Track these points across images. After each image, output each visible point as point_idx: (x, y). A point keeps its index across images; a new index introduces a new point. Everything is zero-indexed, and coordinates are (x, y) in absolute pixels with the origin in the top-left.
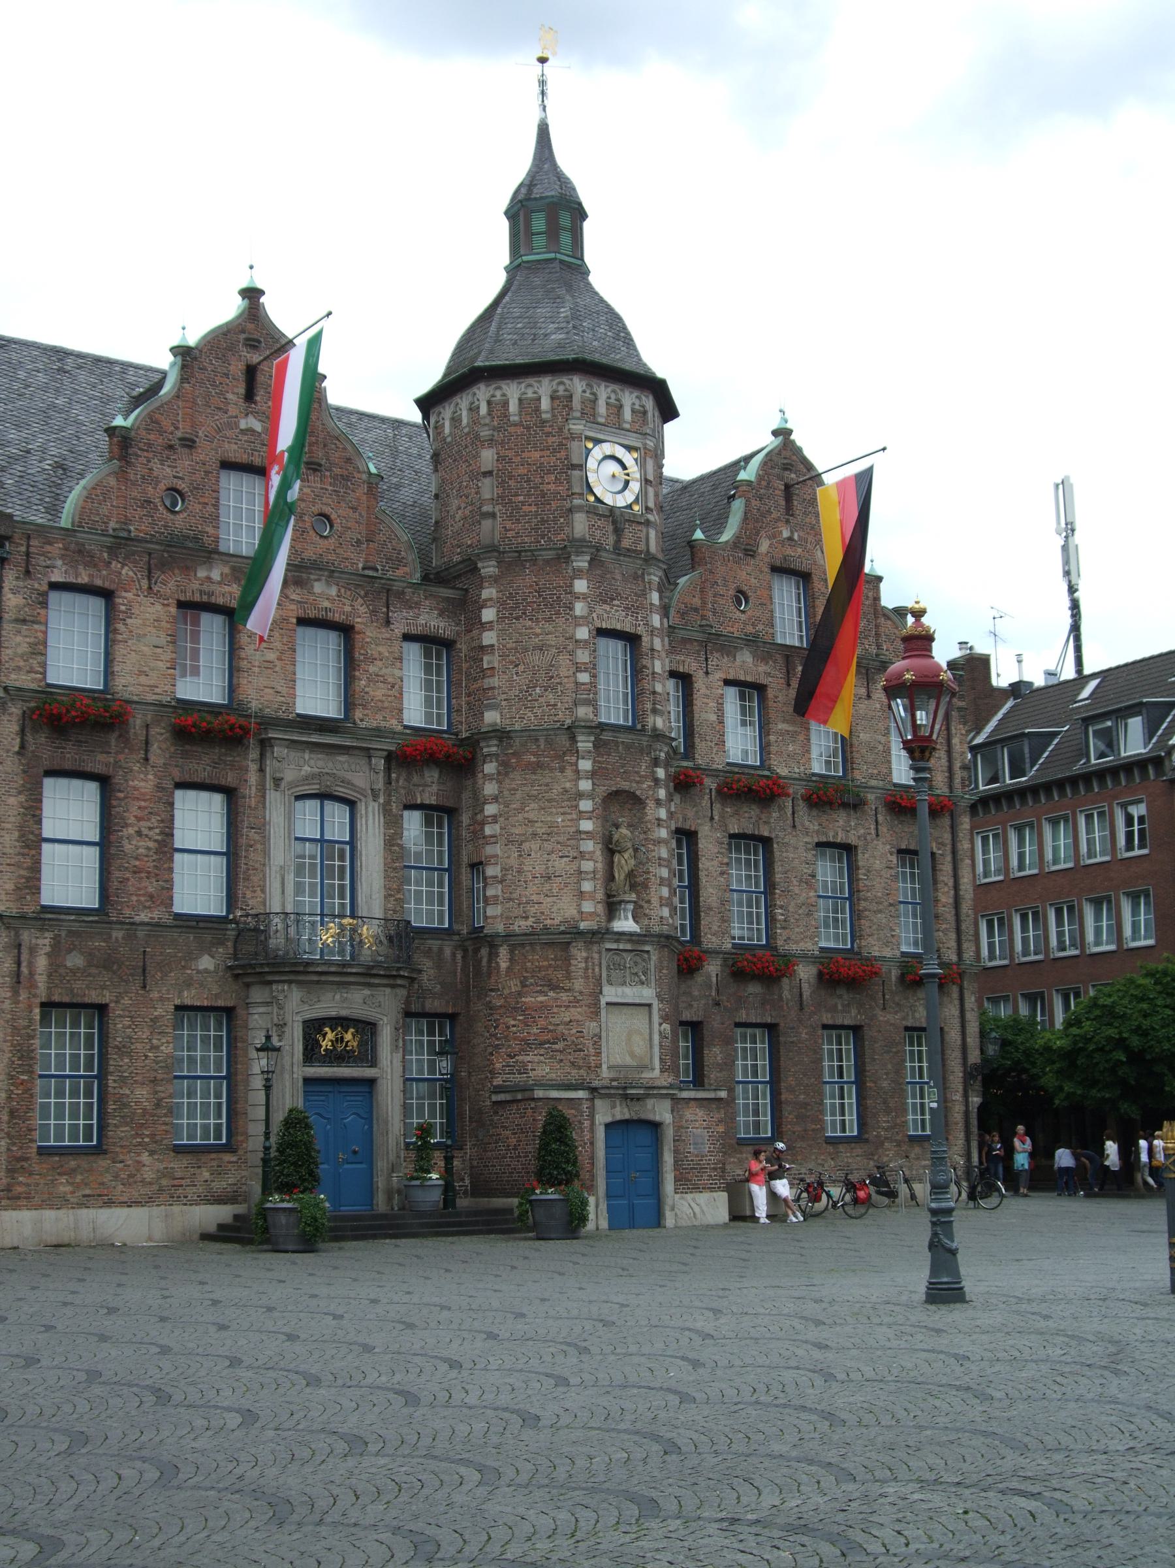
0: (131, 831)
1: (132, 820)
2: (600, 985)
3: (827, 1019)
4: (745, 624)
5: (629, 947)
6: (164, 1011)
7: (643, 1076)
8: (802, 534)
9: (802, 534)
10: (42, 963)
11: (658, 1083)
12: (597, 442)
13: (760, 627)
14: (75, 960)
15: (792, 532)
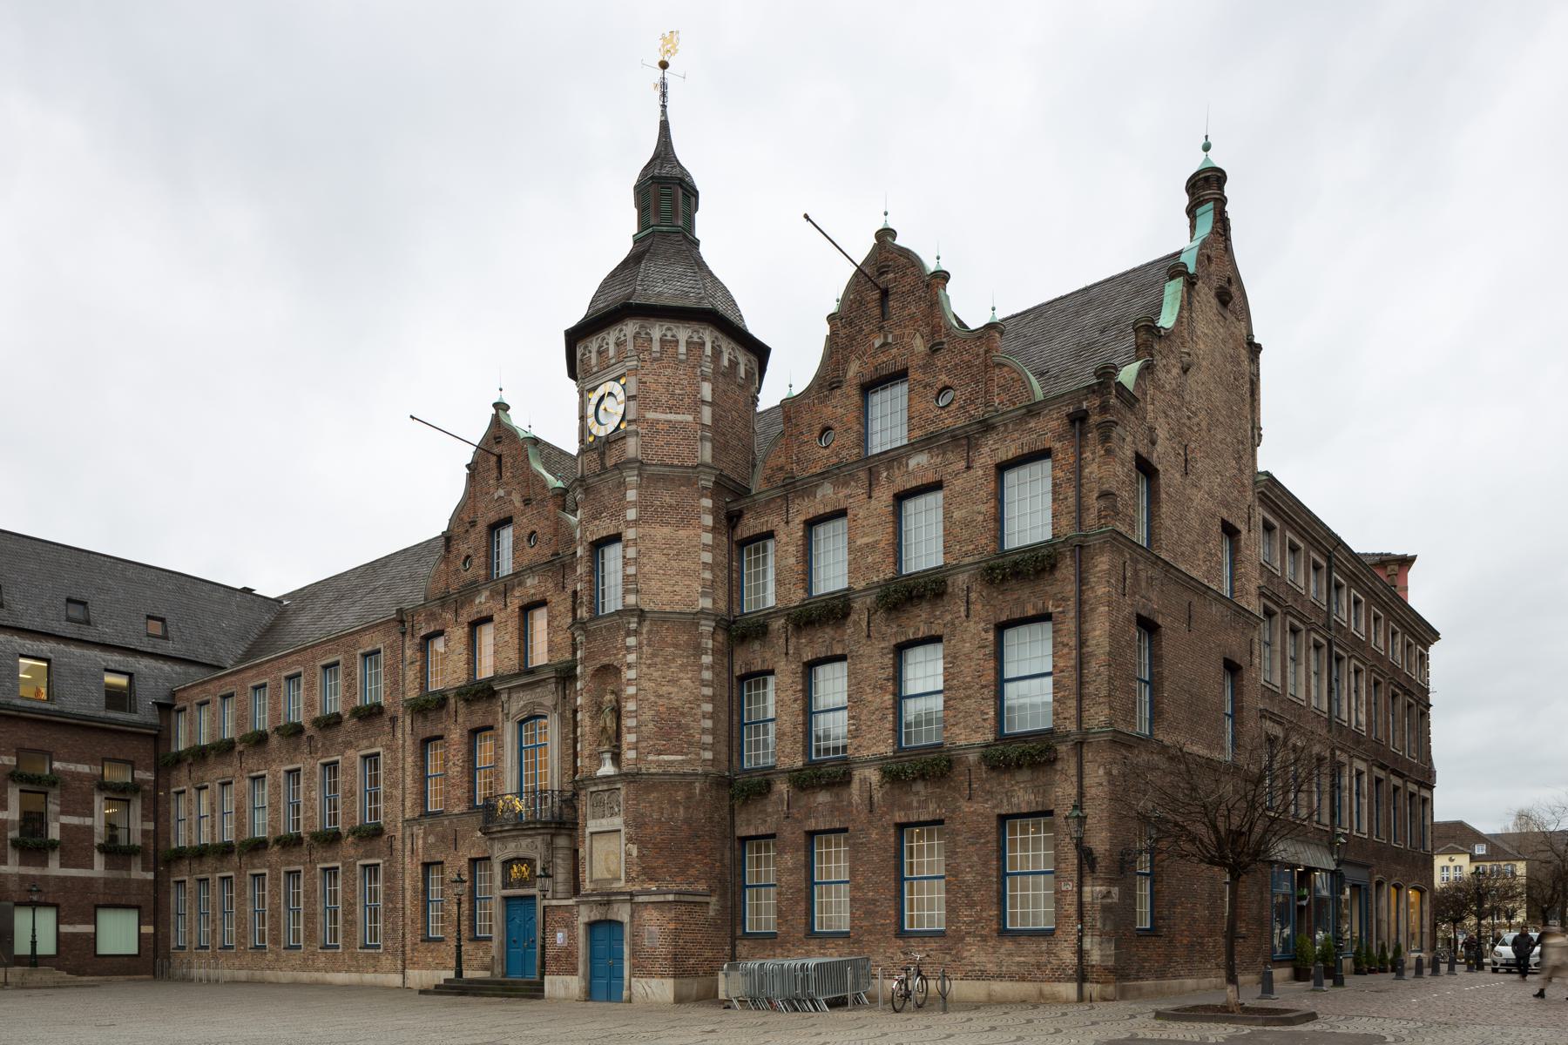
3: (900, 817)
4: (829, 457)
13: (844, 453)
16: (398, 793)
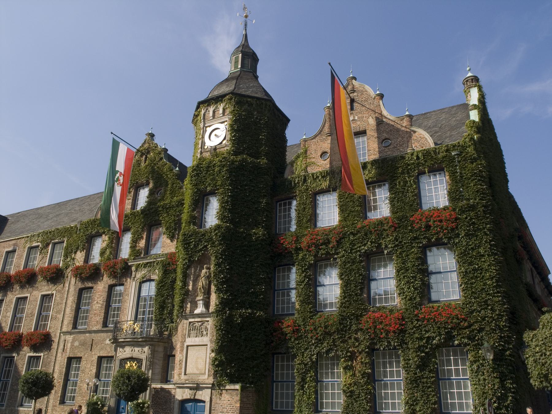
0: (95, 302)
1: (96, 299)
2: (185, 338)
5: (199, 320)
6: (95, 358)
7: (200, 378)
8: (360, 115)
9: (360, 115)
10: (69, 345)
11: (207, 381)
12: (209, 126)
14: (77, 344)
15: (354, 117)
16: (60, 316)
